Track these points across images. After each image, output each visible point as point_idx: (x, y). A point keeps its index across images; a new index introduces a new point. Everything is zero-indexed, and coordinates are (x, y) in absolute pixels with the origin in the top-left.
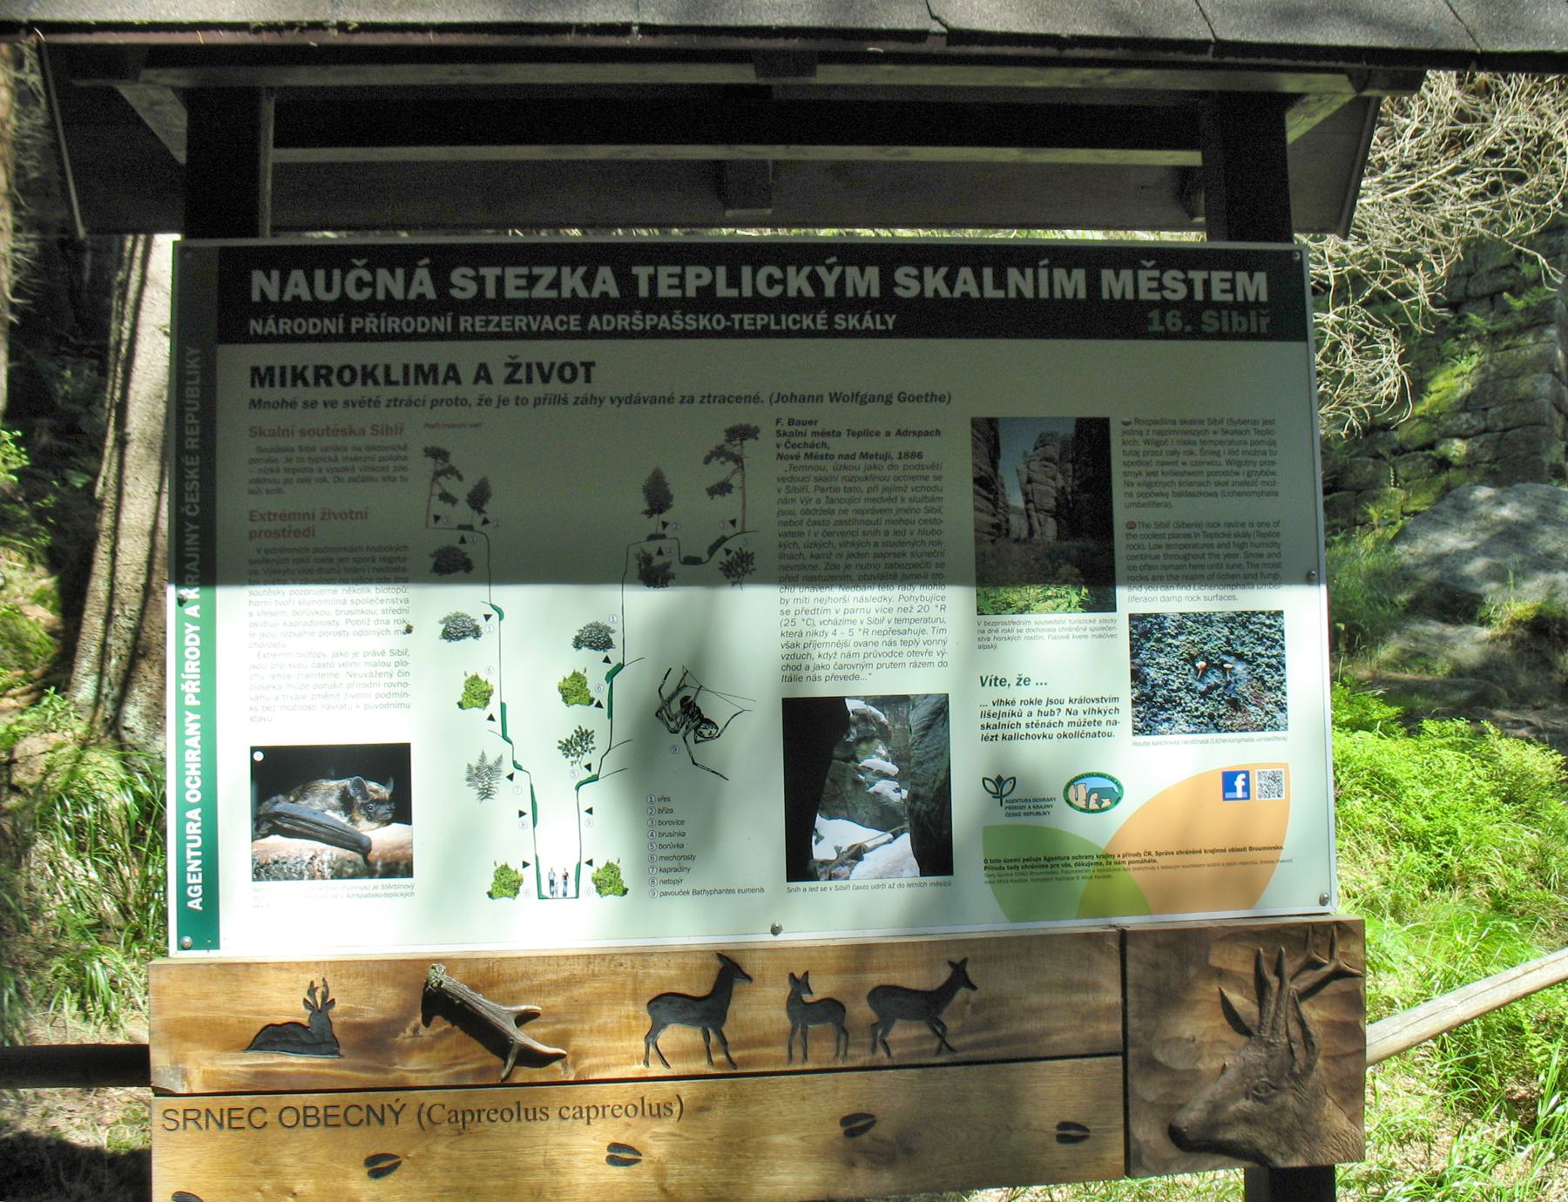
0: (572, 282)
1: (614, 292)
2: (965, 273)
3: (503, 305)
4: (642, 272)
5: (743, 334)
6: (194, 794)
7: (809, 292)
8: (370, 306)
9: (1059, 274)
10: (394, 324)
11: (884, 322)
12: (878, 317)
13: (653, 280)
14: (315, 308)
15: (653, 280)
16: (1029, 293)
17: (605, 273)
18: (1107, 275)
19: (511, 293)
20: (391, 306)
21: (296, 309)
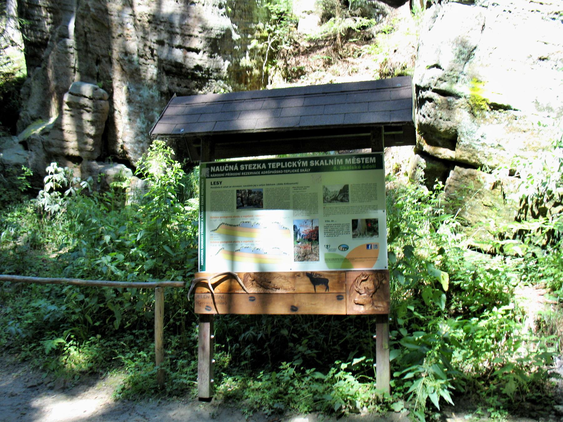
0: (259, 166)
1: (265, 168)
2: (322, 161)
3: (248, 171)
4: (270, 164)
5: (285, 173)
6: (202, 247)
7: (296, 166)
8: (229, 172)
9: (338, 160)
10: (232, 174)
13: (271, 165)
14: (220, 172)
15: (271, 165)
16: (333, 164)
17: (264, 165)
18: (346, 160)
19: (249, 169)
20: (231, 172)
21: (217, 173)
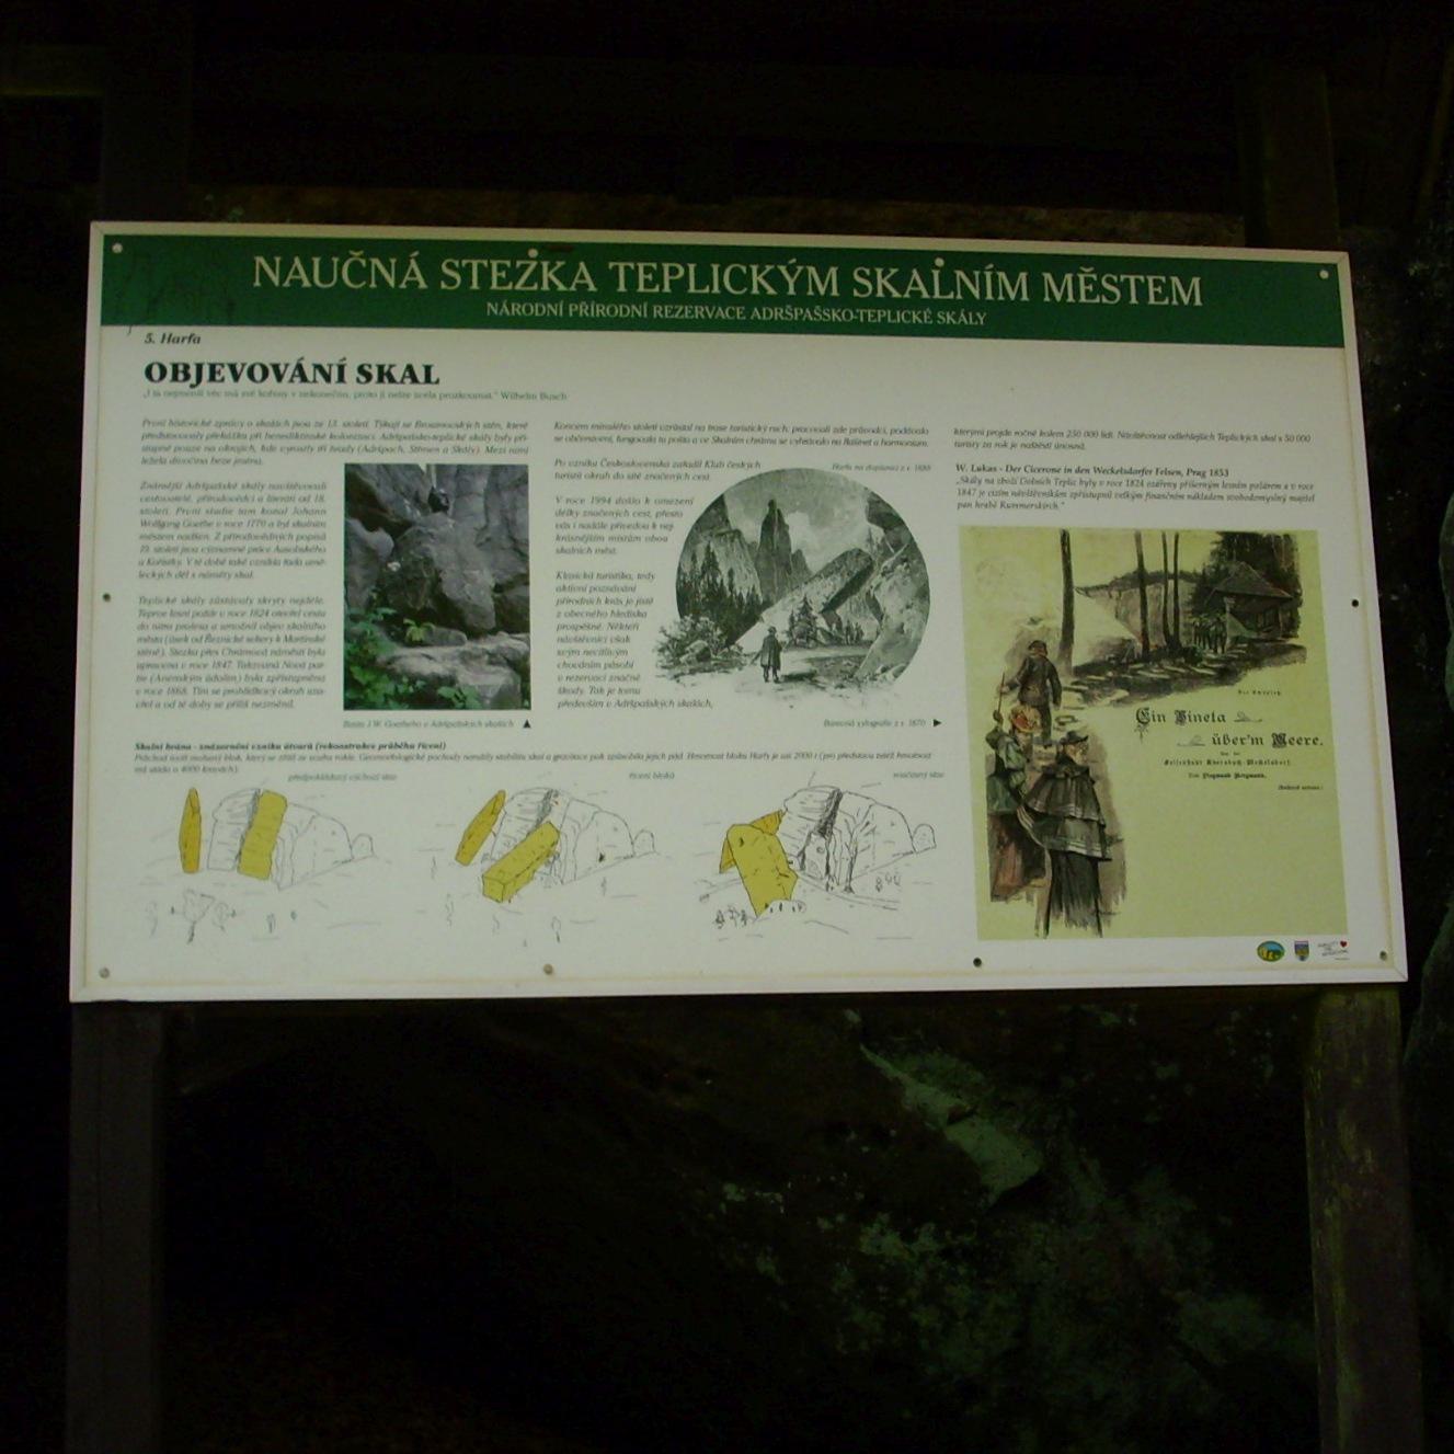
11: (975, 318)
12: (970, 314)
